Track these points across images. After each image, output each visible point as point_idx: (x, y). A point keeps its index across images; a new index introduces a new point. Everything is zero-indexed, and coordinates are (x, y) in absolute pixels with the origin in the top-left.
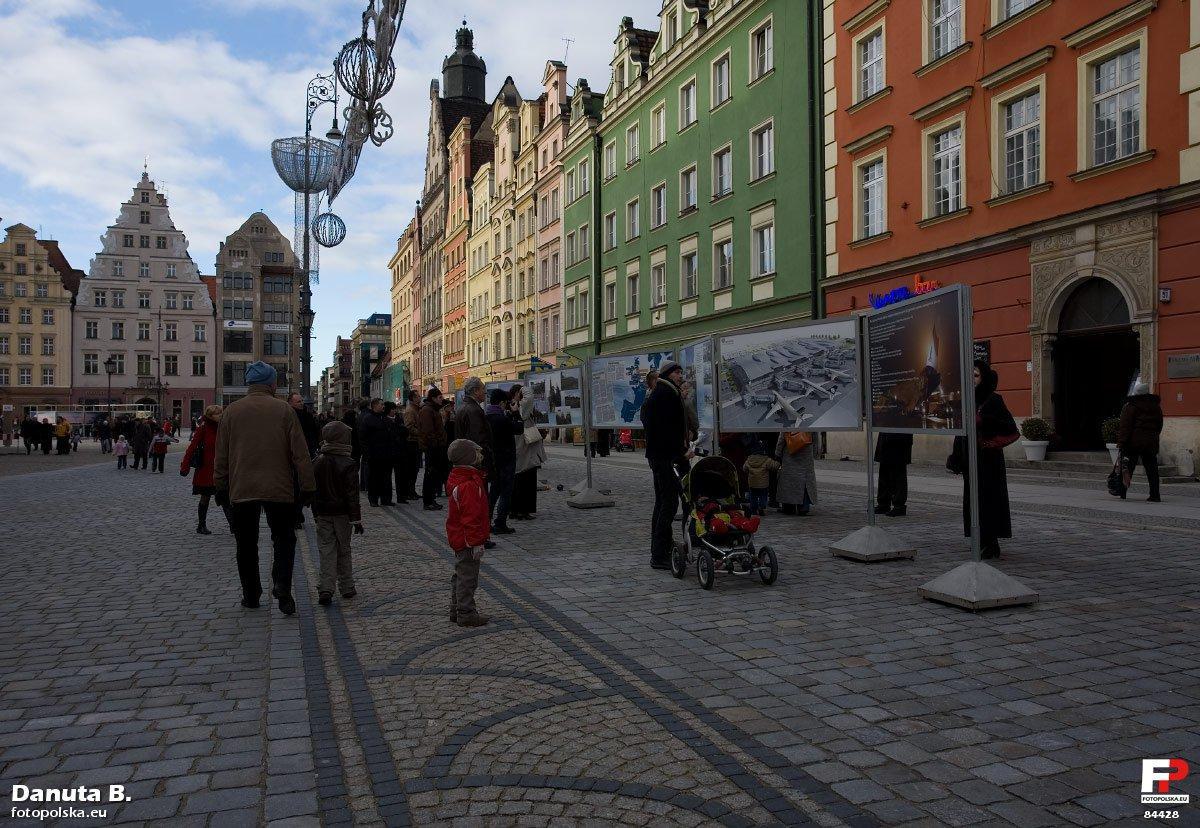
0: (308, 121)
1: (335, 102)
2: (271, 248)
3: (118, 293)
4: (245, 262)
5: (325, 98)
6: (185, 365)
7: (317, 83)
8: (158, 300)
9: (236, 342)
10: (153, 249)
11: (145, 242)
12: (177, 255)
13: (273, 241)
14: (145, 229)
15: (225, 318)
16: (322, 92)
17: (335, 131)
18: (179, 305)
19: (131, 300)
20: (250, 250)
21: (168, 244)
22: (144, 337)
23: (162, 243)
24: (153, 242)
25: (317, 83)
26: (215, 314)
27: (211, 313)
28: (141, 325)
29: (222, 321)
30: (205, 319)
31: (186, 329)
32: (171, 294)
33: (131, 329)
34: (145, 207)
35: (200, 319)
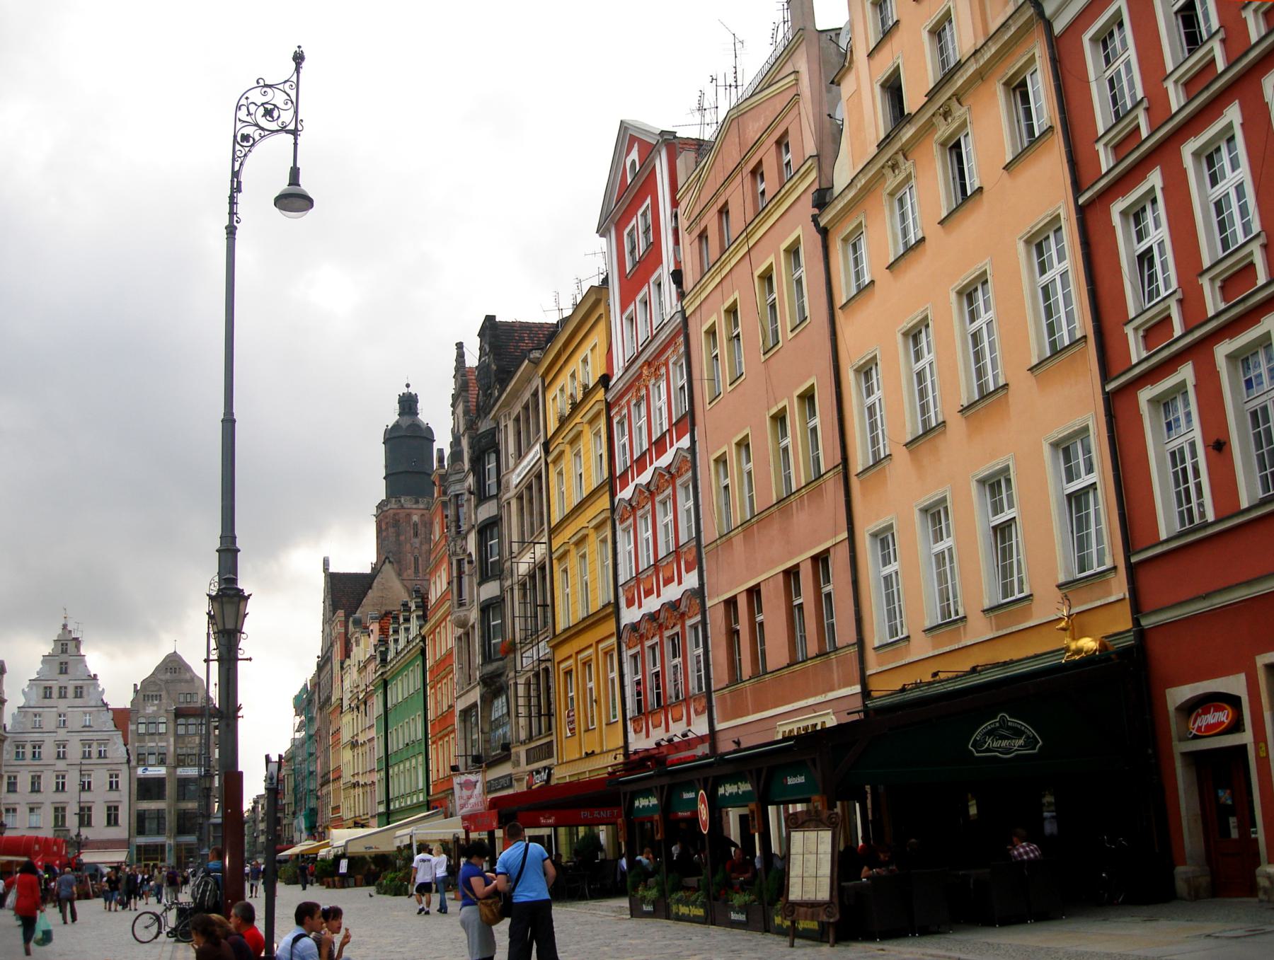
0: (235, 174)
1: (295, 133)
2: (184, 688)
3: (37, 746)
4: (159, 706)
5: (273, 126)
6: (99, 816)
7: (256, 96)
8: (75, 751)
9: (149, 789)
10: (70, 700)
11: (63, 694)
12: (93, 703)
13: (187, 681)
14: (63, 681)
15: (138, 765)
16: (268, 113)
17: (294, 189)
18: (95, 754)
19: (48, 751)
20: (163, 694)
21: (85, 693)
22: (60, 788)
23: (79, 692)
24: (71, 692)
25: (256, 96)
26: (129, 761)
27: (125, 760)
28: (57, 777)
29: (135, 768)
30: (120, 767)
31: (99, 778)
32: (87, 743)
33: (48, 781)
34: (64, 658)
35: (114, 767)
